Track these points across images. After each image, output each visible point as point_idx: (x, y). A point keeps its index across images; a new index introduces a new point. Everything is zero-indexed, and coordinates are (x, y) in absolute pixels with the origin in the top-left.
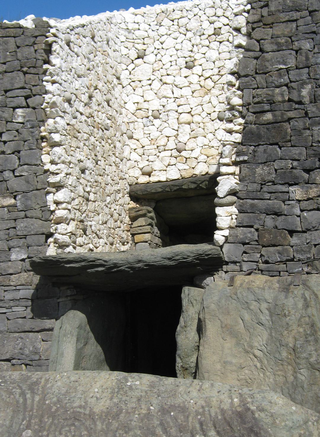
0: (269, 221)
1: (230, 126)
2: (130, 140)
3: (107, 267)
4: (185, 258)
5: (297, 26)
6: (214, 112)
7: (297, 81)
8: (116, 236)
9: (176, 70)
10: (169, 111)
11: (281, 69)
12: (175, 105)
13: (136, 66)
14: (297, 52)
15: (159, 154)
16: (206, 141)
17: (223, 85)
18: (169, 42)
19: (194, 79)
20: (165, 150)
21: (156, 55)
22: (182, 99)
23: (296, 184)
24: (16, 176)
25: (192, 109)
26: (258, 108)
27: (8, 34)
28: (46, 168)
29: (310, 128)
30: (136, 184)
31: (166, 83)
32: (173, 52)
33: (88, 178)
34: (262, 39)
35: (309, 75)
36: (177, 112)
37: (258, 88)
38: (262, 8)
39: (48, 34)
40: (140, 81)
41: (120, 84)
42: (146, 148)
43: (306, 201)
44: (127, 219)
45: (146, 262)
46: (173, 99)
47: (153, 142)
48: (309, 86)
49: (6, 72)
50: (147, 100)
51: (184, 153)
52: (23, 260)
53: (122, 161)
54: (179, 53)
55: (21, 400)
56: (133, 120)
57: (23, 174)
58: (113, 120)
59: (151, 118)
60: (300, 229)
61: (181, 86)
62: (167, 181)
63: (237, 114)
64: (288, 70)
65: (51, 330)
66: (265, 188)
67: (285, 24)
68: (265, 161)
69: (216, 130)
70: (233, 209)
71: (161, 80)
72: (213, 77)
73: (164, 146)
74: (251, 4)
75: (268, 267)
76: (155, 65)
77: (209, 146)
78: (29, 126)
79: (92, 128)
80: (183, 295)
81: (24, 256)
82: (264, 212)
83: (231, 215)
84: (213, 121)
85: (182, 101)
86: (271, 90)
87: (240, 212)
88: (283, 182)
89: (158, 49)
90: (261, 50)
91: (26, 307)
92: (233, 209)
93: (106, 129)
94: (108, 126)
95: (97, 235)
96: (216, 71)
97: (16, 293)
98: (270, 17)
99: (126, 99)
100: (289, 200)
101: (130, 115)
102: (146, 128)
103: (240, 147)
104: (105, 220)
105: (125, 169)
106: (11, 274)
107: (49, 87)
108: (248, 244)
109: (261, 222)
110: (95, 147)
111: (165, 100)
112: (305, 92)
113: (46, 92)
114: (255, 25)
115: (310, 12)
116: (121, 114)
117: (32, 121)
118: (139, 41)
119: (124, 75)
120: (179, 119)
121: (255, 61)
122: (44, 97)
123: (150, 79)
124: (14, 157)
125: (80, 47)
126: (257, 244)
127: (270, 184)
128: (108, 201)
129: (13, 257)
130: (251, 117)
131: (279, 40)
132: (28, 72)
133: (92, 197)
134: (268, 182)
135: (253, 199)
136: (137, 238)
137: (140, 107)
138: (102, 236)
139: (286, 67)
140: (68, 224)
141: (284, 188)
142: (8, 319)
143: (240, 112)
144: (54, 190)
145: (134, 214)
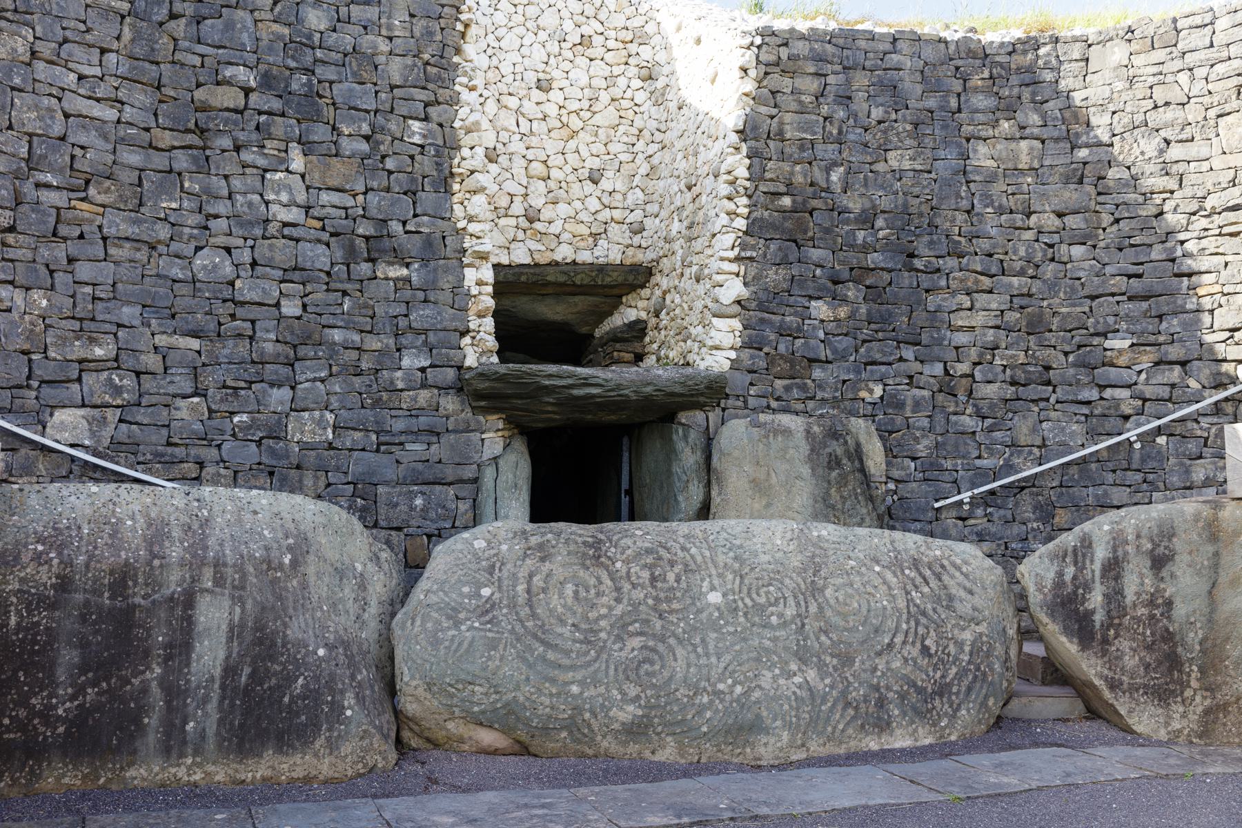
1: (730, 206)
14: (826, 119)
18: (510, 41)
19: (552, 110)
20: (506, 216)
23: (820, 298)
24: (407, 232)
26: (771, 187)
28: (460, 225)
32: (515, 57)
46: (518, 137)
51: (538, 225)
52: (423, 370)
55: (688, 557)
62: (510, 266)
63: (742, 191)
64: (812, 142)
65: (475, 480)
76: (490, 74)
80: (675, 437)
81: (426, 363)
85: (534, 141)
92: (736, 324)
96: (586, 104)
97: (414, 420)
98: (791, 63)
103: (748, 239)
107: (466, 95)
108: (755, 372)
112: (834, 177)
115: (844, 68)
121: (769, 121)
129: (406, 362)
131: (803, 98)
132: (432, 61)
141: (804, 301)
142: (398, 462)
143: (746, 189)
144: (477, 262)
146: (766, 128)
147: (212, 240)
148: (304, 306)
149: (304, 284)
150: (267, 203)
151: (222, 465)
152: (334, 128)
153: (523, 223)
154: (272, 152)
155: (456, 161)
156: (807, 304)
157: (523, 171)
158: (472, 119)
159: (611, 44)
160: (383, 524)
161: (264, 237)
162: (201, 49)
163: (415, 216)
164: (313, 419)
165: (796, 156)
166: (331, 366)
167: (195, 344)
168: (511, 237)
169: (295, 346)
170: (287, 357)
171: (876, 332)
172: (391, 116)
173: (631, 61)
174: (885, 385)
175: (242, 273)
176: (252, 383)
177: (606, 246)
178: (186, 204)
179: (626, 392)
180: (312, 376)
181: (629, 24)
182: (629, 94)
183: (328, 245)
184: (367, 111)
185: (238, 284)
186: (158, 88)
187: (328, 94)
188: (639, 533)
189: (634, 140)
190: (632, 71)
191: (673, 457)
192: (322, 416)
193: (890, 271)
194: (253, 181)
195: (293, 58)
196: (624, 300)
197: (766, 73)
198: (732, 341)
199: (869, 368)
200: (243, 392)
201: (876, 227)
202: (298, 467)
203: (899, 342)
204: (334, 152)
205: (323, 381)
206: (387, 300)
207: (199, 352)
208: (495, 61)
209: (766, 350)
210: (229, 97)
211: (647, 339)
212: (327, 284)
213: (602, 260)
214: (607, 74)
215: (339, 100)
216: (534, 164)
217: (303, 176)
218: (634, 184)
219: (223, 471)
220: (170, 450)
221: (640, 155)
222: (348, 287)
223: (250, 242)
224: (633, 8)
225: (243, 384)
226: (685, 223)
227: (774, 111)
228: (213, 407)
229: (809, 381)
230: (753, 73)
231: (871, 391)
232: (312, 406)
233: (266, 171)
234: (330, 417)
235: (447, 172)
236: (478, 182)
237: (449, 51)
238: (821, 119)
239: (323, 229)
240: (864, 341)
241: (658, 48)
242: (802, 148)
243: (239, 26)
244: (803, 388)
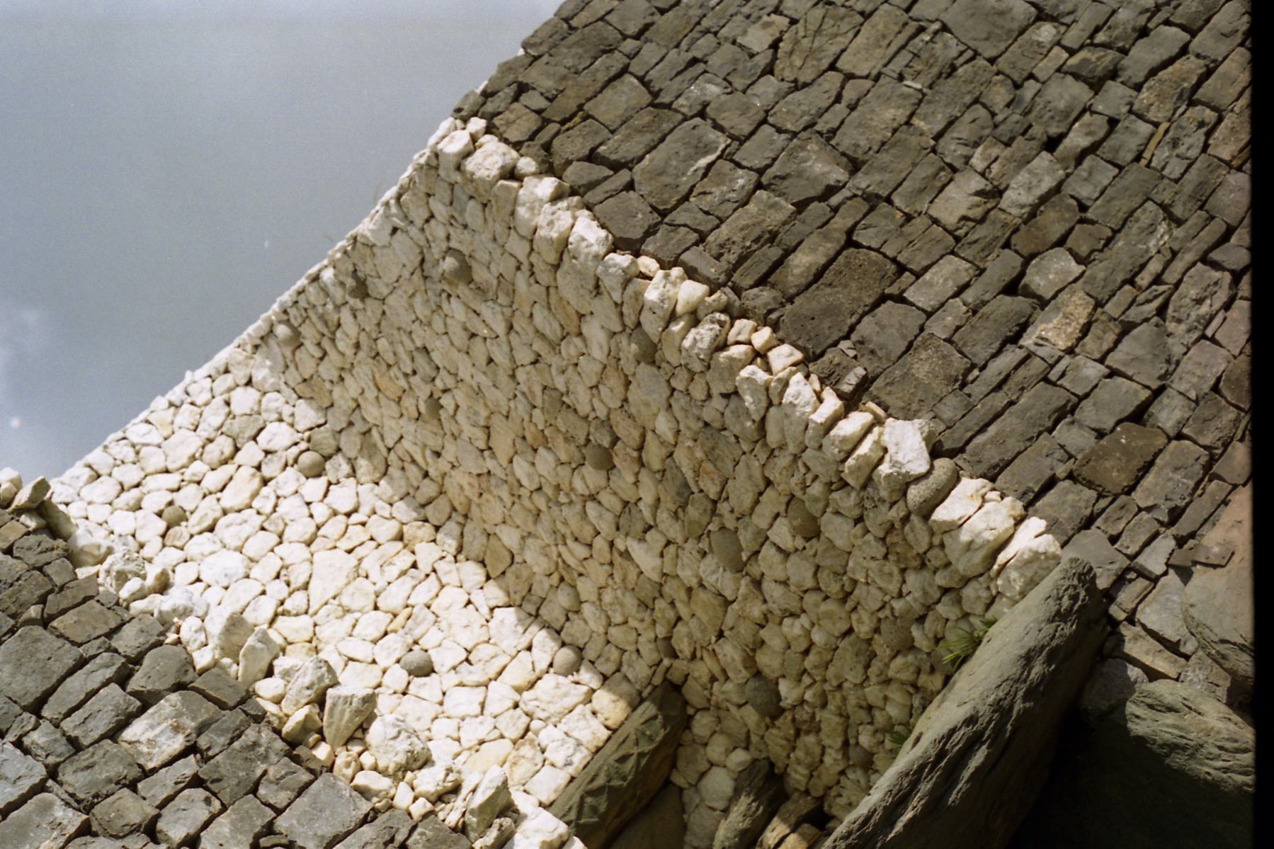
0: (1073, 436)
3: (988, 733)
5: (641, 79)
6: (384, 672)
7: (774, 160)
14: (702, 114)
16: (455, 747)
17: (336, 602)
23: (1023, 328)
35: (786, 131)
45: (1043, 647)
48: (813, 146)
60: (1145, 394)
66: (977, 390)
68: (906, 343)
69: (441, 704)
72: (288, 606)
77: (470, 749)
78: (223, 740)
82: (1036, 431)
83: (984, 500)
84: (404, 694)
86: (738, 218)
87: (992, 476)
88: (997, 345)
90: (616, 167)
92: (969, 486)
96: (278, 590)
100: (1052, 366)
109: (1059, 454)
114: (544, 136)
122: (179, 642)
126: (1110, 499)
130: (764, 296)
132: (51, 608)
135: (983, 429)
139: (718, 153)
141: (1011, 357)
156: (1021, 354)
158: (216, 625)
159: (213, 480)
171: (1157, 280)
172: (84, 758)
173: (266, 471)
177: (557, 733)
179: (1019, 706)
181: (204, 432)
182: (320, 511)
189: (405, 560)
190: (288, 480)
191: (1178, 760)
193: (1057, 189)
196: (678, 779)
203: (1204, 259)
211: (798, 776)
213: (579, 759)
214: (258, 520)
218: (485, 611)
221: (441, 566)
224: (186, 407)
226: (663, 515)
227: (624, 176)
235: (279, 745)
236: (348, 700)
237: (58, 572)
240: (1161, 311)
241: (287, 410)
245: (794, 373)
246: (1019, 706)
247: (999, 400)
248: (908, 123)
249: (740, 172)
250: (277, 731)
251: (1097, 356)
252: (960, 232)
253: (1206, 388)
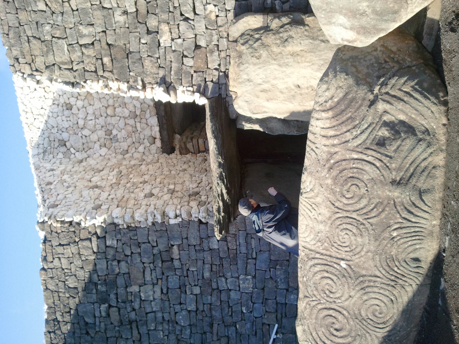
0: (189, 62)
2: (129, 151)
4: (216, 128)
5: (33, 36)
8: (200, 166)
9: (73, 117)
10: (105, 123)
11: (68, 50)
12: (100, 119)
13: (72, 147)
14: (53, 37)
15: (139, 132)
20: (136, 127)
21: (63, 132)
22: (96, 113)
23: (159, 40)
24: (157, 246)
25: (103, 106)
27: (51, 251)
28: (150, 224)
29: (114, 28)
30: (162, 148)
31: (84, 125)
33: (158, 189)
34: (45, 64)
36: (106, 117)
37: (84, 68)
38: (19, 63)
39: (49, 223)
40: (83, 144)
41: (86, 159)
42: (134, 140)
43: (171, 33)
44: (189, 156)
46: (97, 120)
47: (130, 136)
48: (81, 27)
49: (79, 253)
50: (97, 139)
51: (138, 113)
53: (144, 160)
54: (60, 114)
56: (114, 150)
57: (155, 240)
58: (114, 167)
59: (111, 137)
60: (194, 39)
61: (86, 114)
62: (159, 126)
67: (31, 45)
70: (180, 89)
71: (82, 129)
73: (133, 127)
74: (16, 71)
75: (223, 64)
76: (71, 132)
79: (120, 185)
85: (97, 113)
87: (181, 84)
88: (158, 51)
89: (58, 130)
91: (252, 238)
93: (121, 173)
94: (119, 171)
95: (199, 183)
98: (27, 57)
99: (98, 155)
100: (171, 47)
101: (110, 152)
102: (119, 140)
104: (188, 176)
105: (151, 157)
106: (228, 248)
108: (205, 79)
110: (134, 184)
111: (97, 126)
113: (94, 224)
116: (109, 159)
117: (116, 234)
118: (52, 144)
119: (79, 156)
120: (111, 115)
123: (82, 137)
124: (143, 246)
125: (58, 195)
127: (159, 60)
128: (175, 173)
129: (216, 247)
133: (172, 187)
134: (158, 62)
136: (202, 148)
137: (103, 145)
138: (200, 178)
139: (66, 45)
140: (192, 208)
142: (261, 251)
143: (104, 81)
145: (184, 151)
146: (67, 72)
147: (173, 318)
148: (195, 285)
149: (186, 286)
150: (154, 299)
151: (263, 317)
152: (118, 274)
153: (138, 120)
154: (133, 298)
155: (121, 227)
157: (113, 118)
160: (288, 258)
161: (169, 301)
162: (97, 323)
163: (149, 242)
164: (244, 283)
165: (80, 54)
166: (220, 276)
167: (215, 326)
168: (146, 126)
169: (213, 290)
170: (218, 293)
172: (107, 253)
174: (207, 3)
175: (185, 308)
176: (229, 306)
178: (161, 329)
180: (225, 284)
183: (168, 276)
184: (107, 262)
185: (189, 309)
186: (117, 338)
187: (103, 278)
188: (305, 279)
192: (241, 279)
194: (146, 305)
195: (92, 290)
197: (37, 70)
198: (189, 93)
199: (197, 12)
200: (233, 309)
201: (111, 7)
202: (263, 289)
204: (128, 275)
205: (226, 279)
206: (189, 254)
207: (218, 324)
208: (64, 130)
209: (192, 72)
210: (114, 311)
212: (185, 277)
215: (105, 273)
216: (109, 113)
217: (140, 286)
219: (266, 317)
220: (258, 335)
222: (185, 269)
223: (172, 305)
225: (230, 309)
228: (240, 319)
229: (208, 49)
230: (38, 78)
231: (211, 12)
232: (237, 284)
233: (141, 299)
234: (242, 277)
235: (127, 230)
238: (54, 39)
239: (161, 279)
240: (182, 15)
242: (74, 51)
243: (84, 309)
244: (212, 52)
245: (129, 91)
246: (224, 174)
247: (168, 63)
248: (92, 5)
249: (74, 46)
250: (124, 228)
251: (178, 37)
252: (127, 26)
253: (205, 30)
